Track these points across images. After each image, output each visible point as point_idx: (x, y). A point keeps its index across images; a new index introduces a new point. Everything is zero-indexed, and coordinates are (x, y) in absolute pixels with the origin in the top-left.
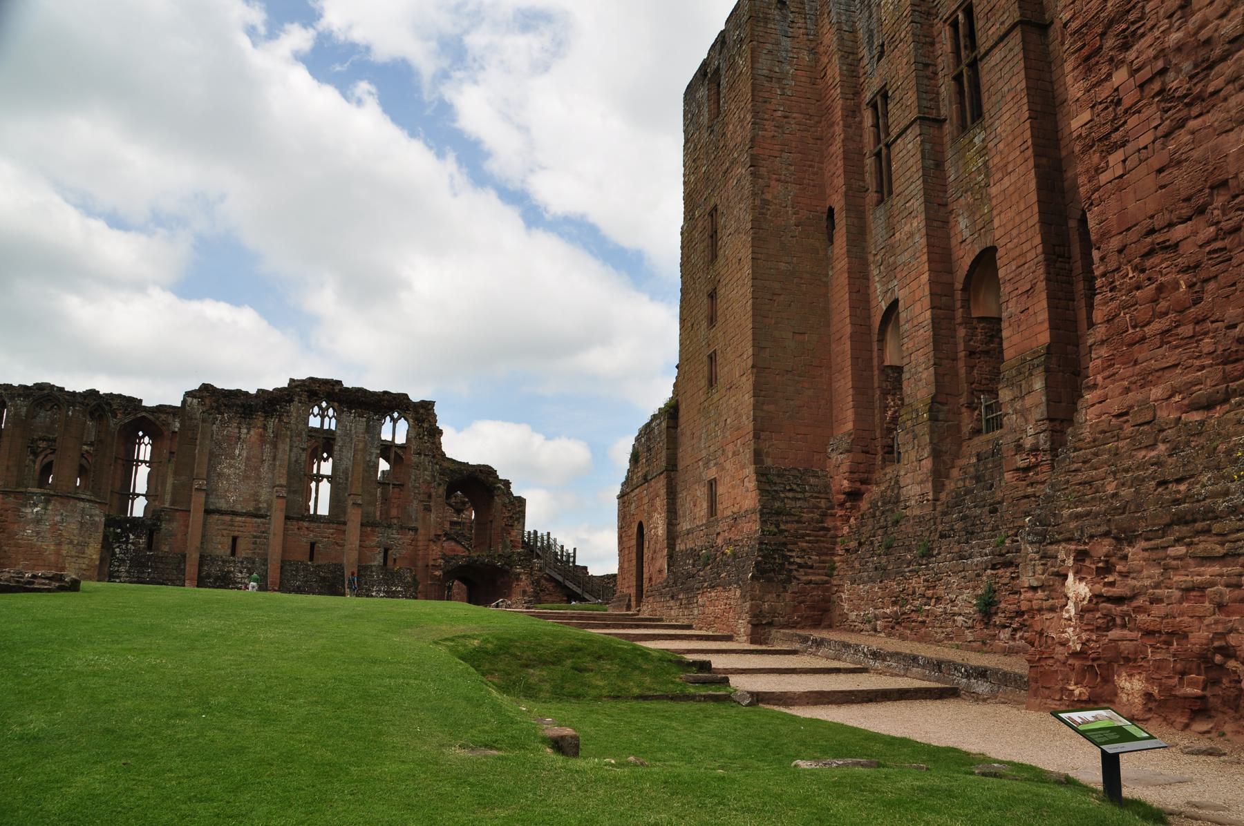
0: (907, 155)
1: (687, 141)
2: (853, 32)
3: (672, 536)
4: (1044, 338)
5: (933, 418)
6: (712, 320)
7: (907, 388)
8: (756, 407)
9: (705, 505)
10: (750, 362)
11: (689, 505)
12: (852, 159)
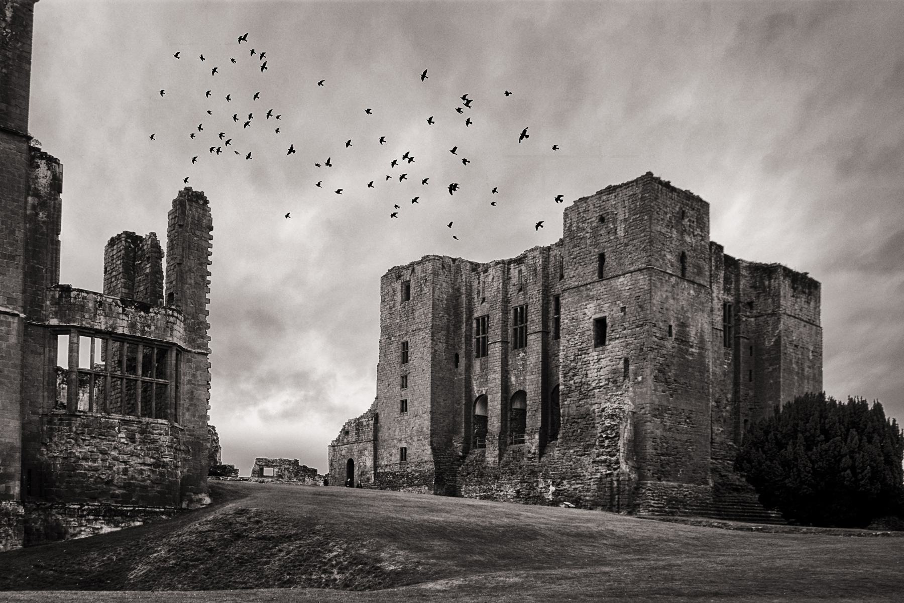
0: (495, 350)
2: (471, 286)
3: (376, 466)
4: (539, 424)
5: (500, 439)
6: (404, 385)
7: (489, 427)
8: (432, 426)
9: (398, 457)
10: (429, 410)
11: (386, 454)
12: (468, 338)
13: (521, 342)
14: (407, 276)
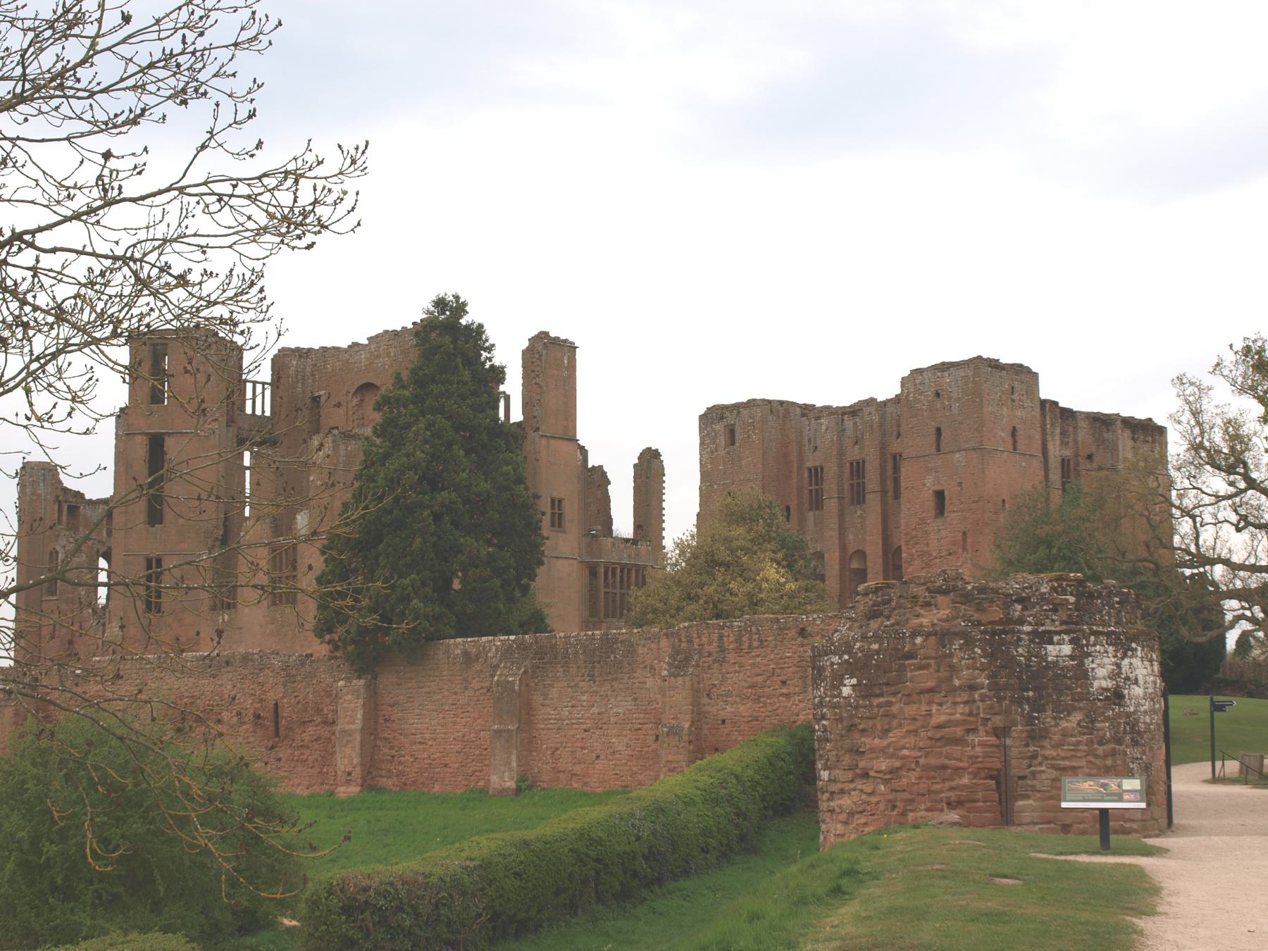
0: (831, 505)
1: (702, 444)
13: (858, 496)
14: (731, 419)
